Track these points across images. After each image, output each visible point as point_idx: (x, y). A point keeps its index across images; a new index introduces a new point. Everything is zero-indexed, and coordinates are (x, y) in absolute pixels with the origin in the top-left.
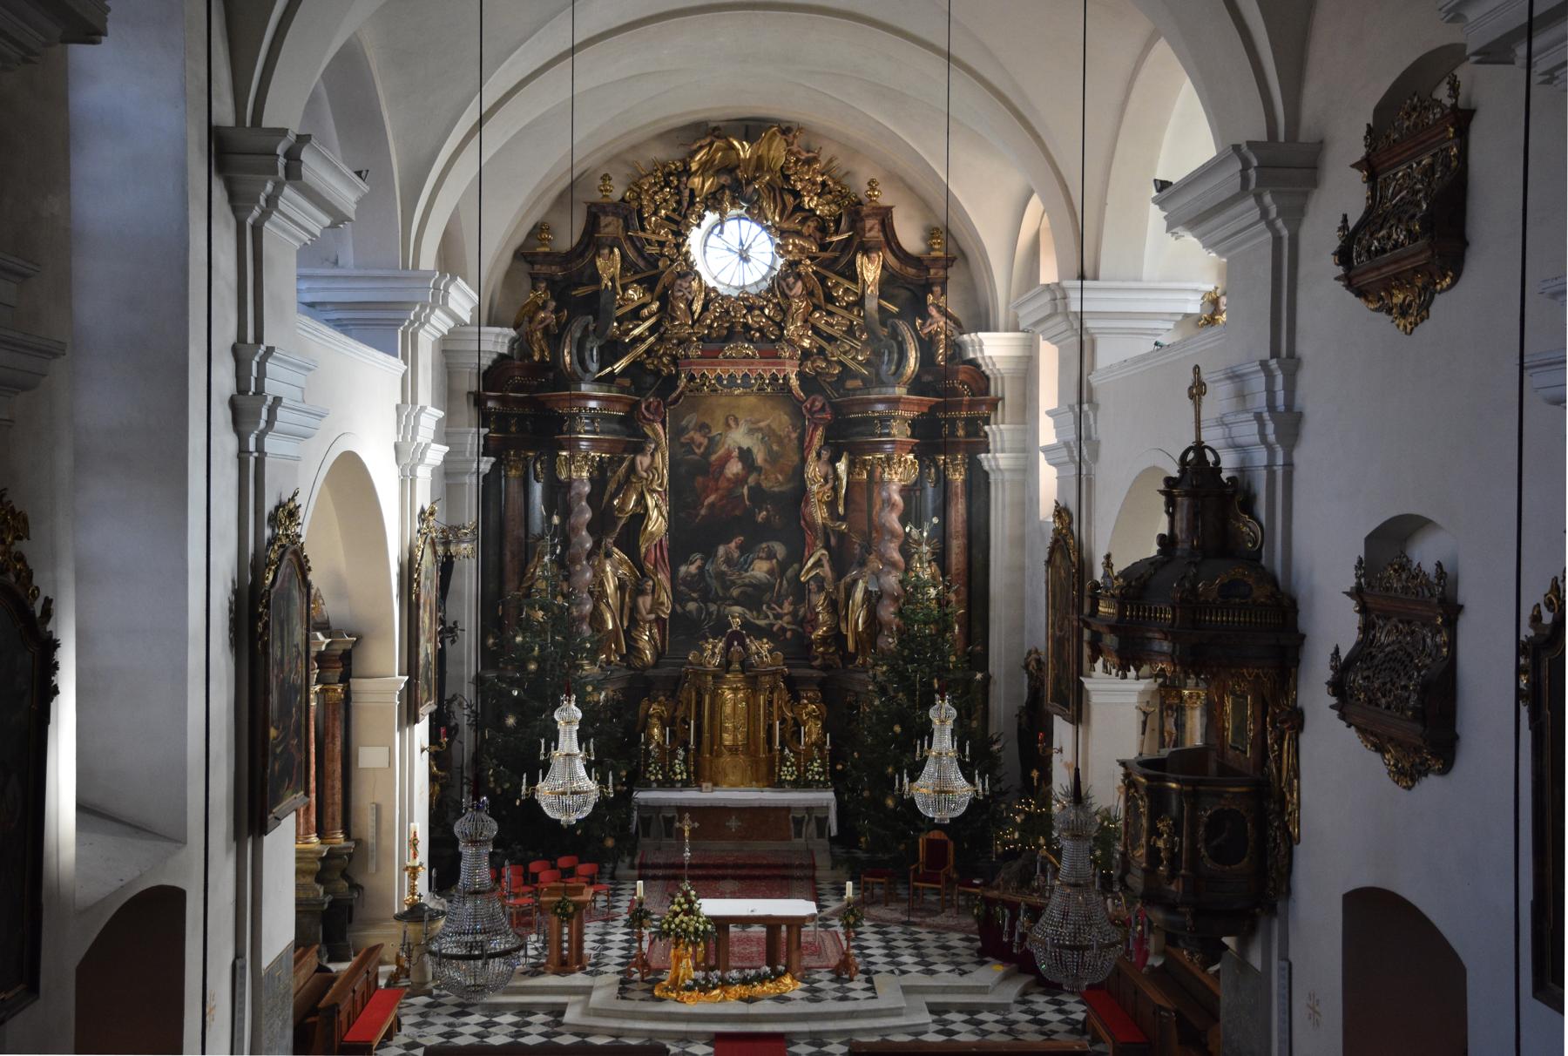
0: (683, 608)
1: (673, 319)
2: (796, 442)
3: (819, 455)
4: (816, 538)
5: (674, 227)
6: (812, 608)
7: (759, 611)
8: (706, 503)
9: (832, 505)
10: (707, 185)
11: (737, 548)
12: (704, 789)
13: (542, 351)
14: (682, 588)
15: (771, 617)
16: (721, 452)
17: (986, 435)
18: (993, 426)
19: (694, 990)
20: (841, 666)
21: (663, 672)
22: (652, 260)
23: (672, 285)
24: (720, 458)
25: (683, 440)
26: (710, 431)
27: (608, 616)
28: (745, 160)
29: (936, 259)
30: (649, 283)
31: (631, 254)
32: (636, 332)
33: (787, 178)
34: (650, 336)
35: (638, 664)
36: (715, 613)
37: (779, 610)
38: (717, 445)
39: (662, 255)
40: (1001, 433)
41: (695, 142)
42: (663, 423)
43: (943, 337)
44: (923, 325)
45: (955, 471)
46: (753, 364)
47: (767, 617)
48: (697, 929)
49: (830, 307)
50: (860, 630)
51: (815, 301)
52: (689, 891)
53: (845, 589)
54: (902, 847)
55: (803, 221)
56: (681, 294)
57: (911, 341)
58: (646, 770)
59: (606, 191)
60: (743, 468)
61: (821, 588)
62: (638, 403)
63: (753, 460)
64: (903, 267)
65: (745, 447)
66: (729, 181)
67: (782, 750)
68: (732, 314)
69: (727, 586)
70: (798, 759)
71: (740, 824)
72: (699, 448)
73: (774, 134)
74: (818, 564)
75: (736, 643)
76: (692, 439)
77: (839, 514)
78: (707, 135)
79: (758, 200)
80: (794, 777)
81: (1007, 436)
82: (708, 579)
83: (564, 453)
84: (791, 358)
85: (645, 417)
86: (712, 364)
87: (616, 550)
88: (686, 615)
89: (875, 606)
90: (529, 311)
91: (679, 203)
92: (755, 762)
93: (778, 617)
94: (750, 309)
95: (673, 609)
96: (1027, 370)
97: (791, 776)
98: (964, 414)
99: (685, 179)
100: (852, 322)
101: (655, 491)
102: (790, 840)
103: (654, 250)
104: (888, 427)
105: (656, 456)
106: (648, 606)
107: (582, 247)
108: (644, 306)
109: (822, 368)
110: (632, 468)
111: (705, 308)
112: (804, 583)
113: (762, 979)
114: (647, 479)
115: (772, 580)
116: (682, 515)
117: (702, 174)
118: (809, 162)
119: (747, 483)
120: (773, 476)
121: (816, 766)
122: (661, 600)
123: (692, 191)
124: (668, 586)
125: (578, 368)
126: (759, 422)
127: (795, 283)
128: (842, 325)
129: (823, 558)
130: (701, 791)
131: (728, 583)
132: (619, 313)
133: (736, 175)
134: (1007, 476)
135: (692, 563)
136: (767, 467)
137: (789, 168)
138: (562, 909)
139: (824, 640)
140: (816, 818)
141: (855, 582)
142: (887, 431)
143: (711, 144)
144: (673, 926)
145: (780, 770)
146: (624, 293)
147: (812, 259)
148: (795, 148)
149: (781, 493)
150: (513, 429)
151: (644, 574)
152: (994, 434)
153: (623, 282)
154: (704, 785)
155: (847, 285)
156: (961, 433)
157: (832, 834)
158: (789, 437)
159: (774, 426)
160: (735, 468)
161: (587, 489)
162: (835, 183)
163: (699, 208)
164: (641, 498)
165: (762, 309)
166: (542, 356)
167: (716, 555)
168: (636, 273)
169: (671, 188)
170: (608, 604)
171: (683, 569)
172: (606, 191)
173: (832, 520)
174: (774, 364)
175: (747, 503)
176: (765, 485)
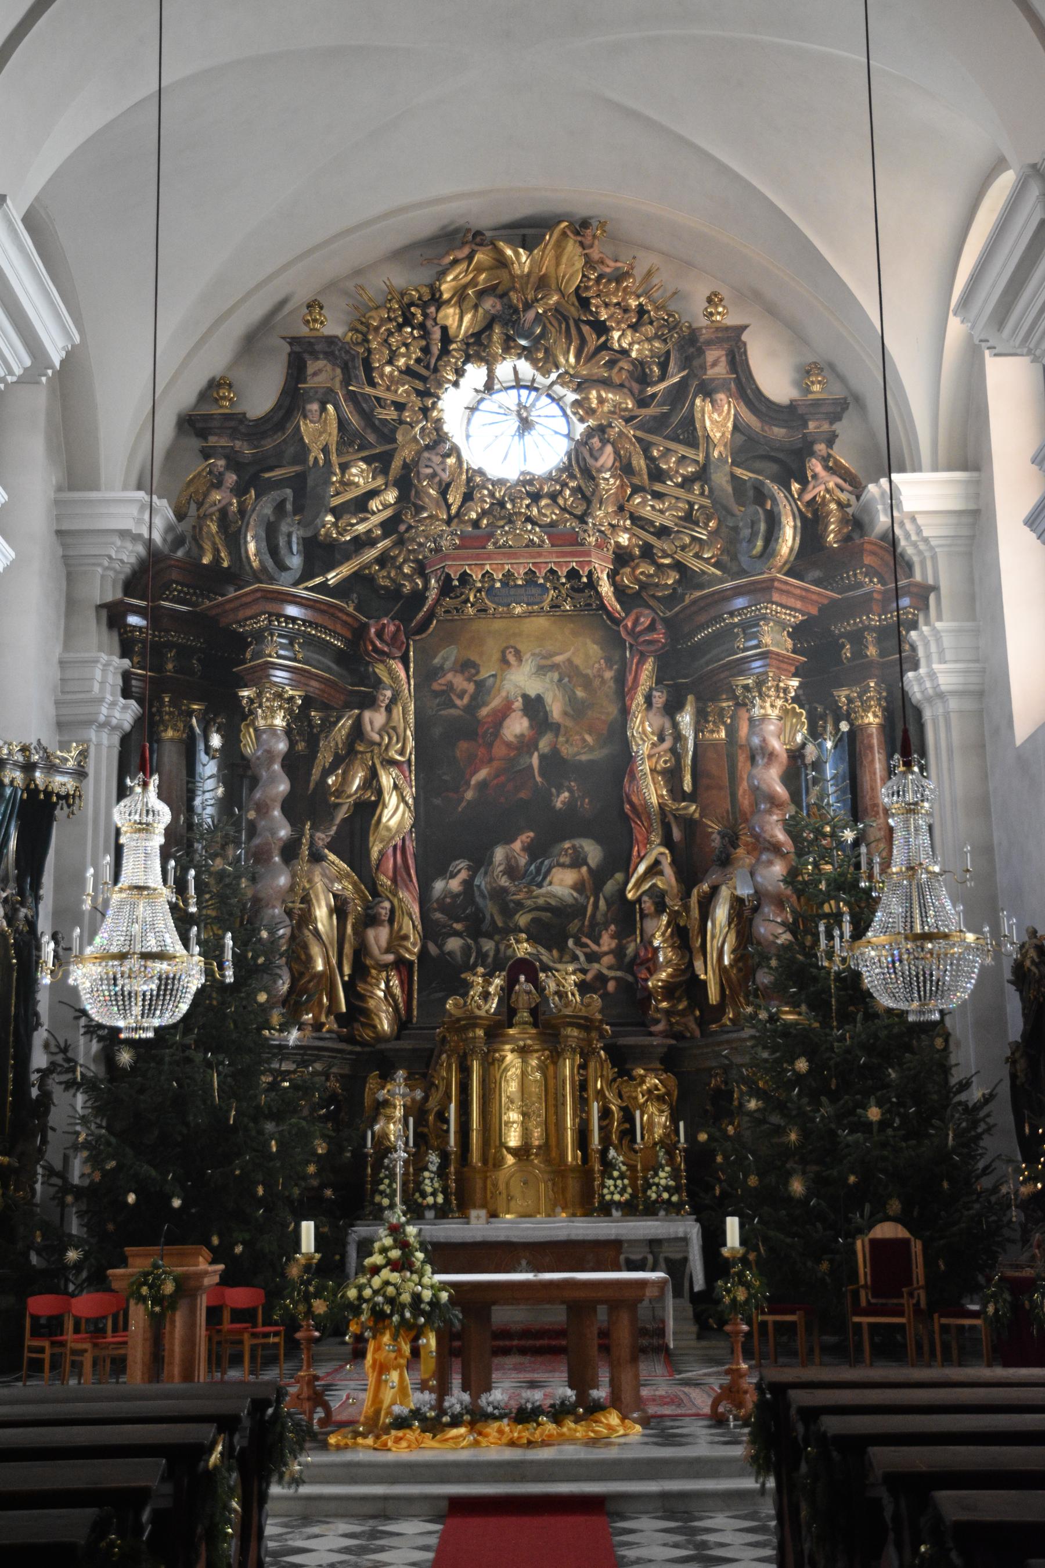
1: (419, 509)
2: (612, 684)
3: (649, 700)
4: (649, 832)
5: (420, 386)
6: (647, 942)
7: (562, 949)
8: (473, 782)
9: (672, 776)
10: (467, 318)
12: (473, 1220)
13: (216, 551)
14: (438, 915)
15: (582, 958)
16: (496, 703)
17: (913, 648)
18: (925, 629)
19: (410, 1427)
20: (698, 1033)
21: (405, 1044)
22: (386, 431)
23: (416, 462)
24: (494, 712)
25: (435, 686)
26: (478, 672)
27: (316, 950)
28: (522, 277)
29: (817, 403)
30: (381, 462)
31: (354, 421)
32: (361, 528)
33: (585, 303)
34: (385, 536)
35: (367, 1035)
36: (492, 954)
37: (594, 947)
38: (489, 692)
39: (401, 422)
40: (938, 640)
41: (447, 253)
42: (405, 661)
43: (833, 506)
44: (801, 492)
45: (867, 709)
46: (540, 555)
47: (575, 958)
48: (417, 1298)
49: (658, 487)
50: (726, 962)
51: (636, 481)
52: (403, 1225)
53: (699, 902)
54: (825, 1266)
55: (611, 364)
56: (429, 471)
57: (785, 502)
58: (375, 1191)
59: (315, 321)
60: (531, 726)
61: (661, 907)
62: (365, 627)
63: (546, 713)
64: (766, 428)
65: (532, 694)
66: (499, 307)
67: (604, 1152)
68: (509, 506)
69: (509, 910)
70: (632, 1168)
72: (461, 697)
73: (564, 234)
74: (654, 869)
75: (522, 978)
76: (450, 685)
77: (684, 792)
78: (464, 244)
79: (542, 335)
80: (626, 1196)
81: (947, 641)
82: (479, 900)
83: (246, 694)
84: (598, 546)
85: (376, 649)
86: (478, 557)
87: (332, 857)
88: (445, 957)
89: (751, 920)
90: (196, 492)
91: (426, 350)
92: (558, 1170)
93: (593, 957)
94: (536, 497)
95: (423, 954)
96: (972, 537)
98: (875, 620)
99: (432, 309)
100: (691, 505)
101: (393, 763)
103: (391, 414)
104: (755, 636)
105: (395, 712)
107: (281, 413)
108: (373, 494)
109: (649, 576)
110: (357, 731)
111: (468, 497)
112: (632, 903)
113: (559, 1413)
114: (379, 745)
115: (581, 900)
116: (437, 801)
117: (460, 303)
118: (619, 277)
119: (537, 749)
120: (577, 737)
121: (663, 1177)
122: (403, 932)
123: (444, 329)
124: (415, 909)
125: (270, 563)
127: (601, 449)
128: (678, 509)
129: (662, 859)
131: (512, 905)
132: (335, 502)
133: (510, 300)
134: (953, 704)
135: (453, 876)
136: (569, 723)
137: (587, 288)
138: (151, 1287)
139: (669, 990)
141: (715, 890)
142: (754, 642)
143: (470, 258)
144: (367, 1293)
145: (603, 1186)
146: (343, 472)
147: (628, 420)
148: (595, 254)
149: (591, 762)
150: (170, 666)
151: (375, 894)
152: (927, 644)
153: (344, 460)
154: (473, 1213)
155: (682, 450)
156: (872, 651)
157: (697, 1289)
158: (602, 677)
159: (578, 661)
160: (517, 726)
161: (282, 746)
162: (657, 309)
163: (456, 357)
164: (372, 780)
165: (554, 497)
166: (217, 559)
167: (491, 863)
168: (361, 448)
169: (413, 328)
170: (316, 933)
171: (439, 886)
172: (315, 321)
173: (674, 800)
174: (573, 554)
175: (539, 779)
176: (566, 751)
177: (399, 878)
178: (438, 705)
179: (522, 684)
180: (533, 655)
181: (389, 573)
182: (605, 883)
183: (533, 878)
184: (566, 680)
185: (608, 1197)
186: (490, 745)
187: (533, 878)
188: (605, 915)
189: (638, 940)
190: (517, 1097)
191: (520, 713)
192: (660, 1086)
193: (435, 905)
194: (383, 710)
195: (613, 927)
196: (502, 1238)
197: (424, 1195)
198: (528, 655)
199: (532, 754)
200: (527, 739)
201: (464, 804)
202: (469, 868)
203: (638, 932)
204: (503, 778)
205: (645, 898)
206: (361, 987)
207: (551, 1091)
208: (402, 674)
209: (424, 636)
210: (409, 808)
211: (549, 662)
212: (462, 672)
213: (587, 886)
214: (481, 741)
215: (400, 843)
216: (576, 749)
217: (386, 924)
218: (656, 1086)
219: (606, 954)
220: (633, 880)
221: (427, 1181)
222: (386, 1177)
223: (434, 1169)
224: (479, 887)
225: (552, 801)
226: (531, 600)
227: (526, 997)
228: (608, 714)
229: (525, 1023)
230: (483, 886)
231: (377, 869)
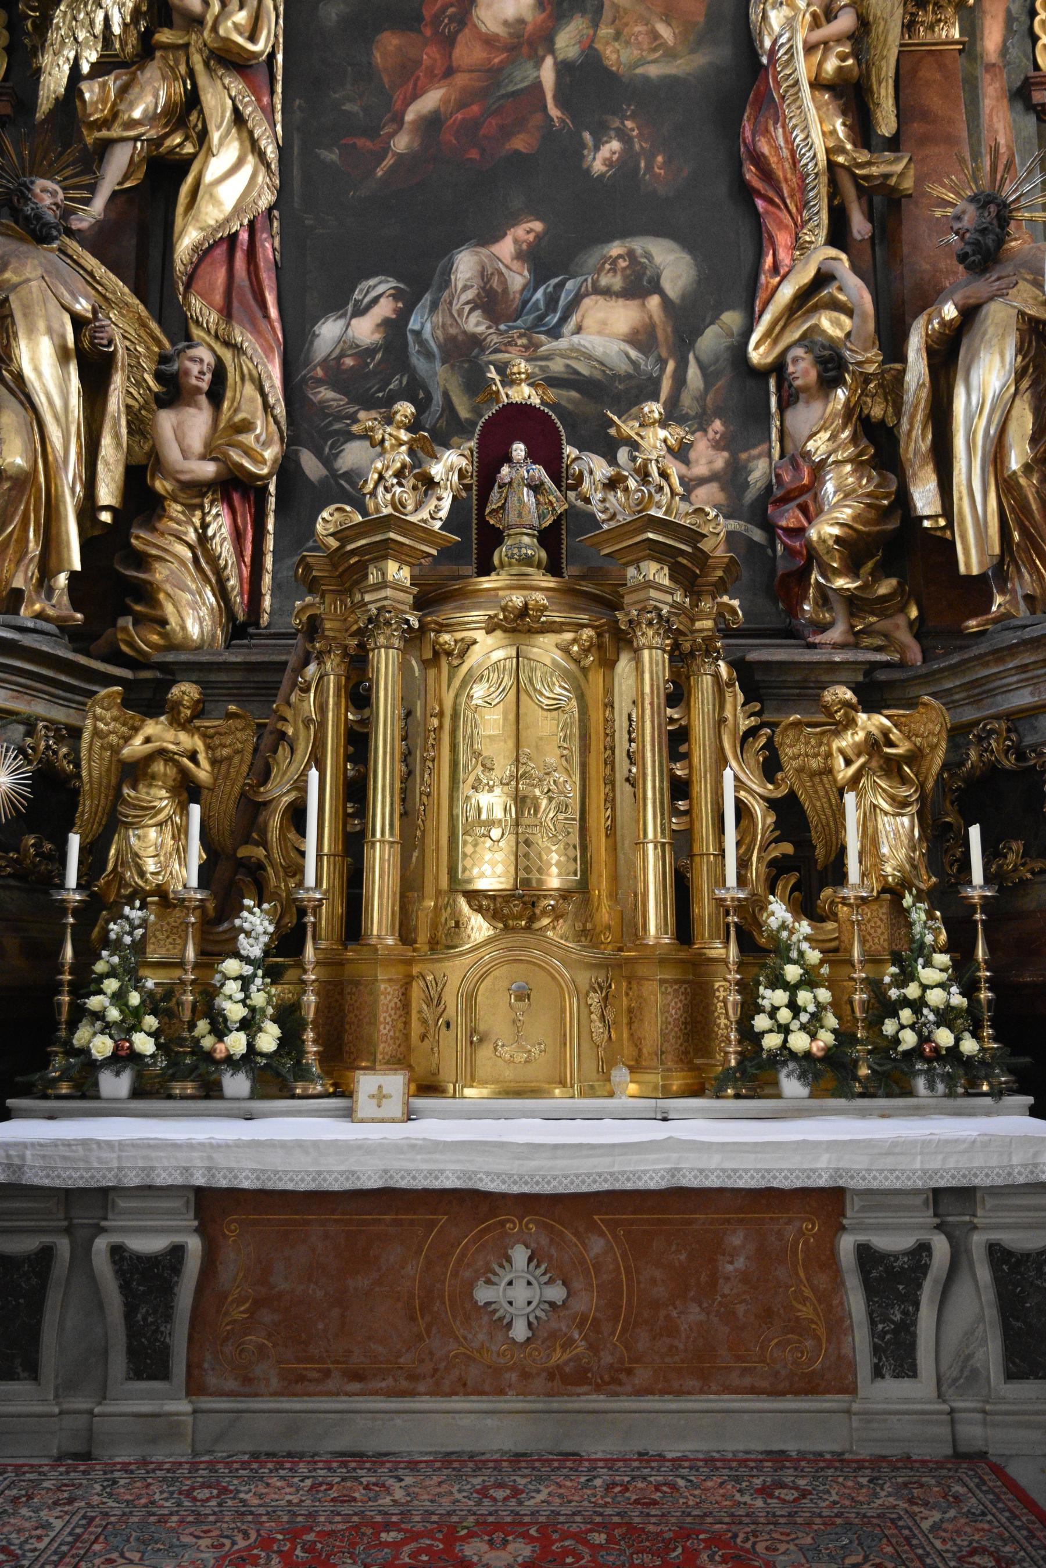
0: (328, 462)
8: (410, 116)
11: (519, 256)
12: (364, 1103)
14: (326, 394)
20: (915, 654)
50: (1015, 463)
58: (79, 1014)
71: (556, 1293)
75: (519, 450)
80: (826, 1038)
82: (419, 363)
97: (811, 1030)
102: (851, 1390)
106: (196, 441)
112: (760, 374)
115: (648, 365)
116: (332, 156)
119: (551, 50)
120: (639, 28)
124: (274, 373)
130: (349, 1114)
135: (360, 311)
140: (997, 1254)
141: (969, 314)
145: (750, 1007)
149: (670, 83)
154: (366, 1083)
167: (446, 283)
175: (554, 112)
177: (235, 304)
182: (700, 332)
183: (541, 318)
185: (772, 1041)
186: (449, 42)
187: (541, 318)
188: (701, 398)
189: (776, 453)
190: (501, 754)
192: (895, 735)
193: (320, 372)
195: (717, 425)
196: (450, 1182)
197: (220, 1029)
199: (543, 59)
200: (529, 28)
201: (389, 161)
202: (397, 295)
203: (774, 434)
204: (475, 108)
205: (799, 352)
206: (140, 539)
207: (597, 744)
210: (268, 166)
213: (660, 335)
214: (428, 32)
215: (244, 236)
216: (636, 52)
217: (203, 399)
218: (886, 733)
219: (702, 481)
221: (232, 988)
222: (112, 973)
223: (256, 951)
224: (418, 334)
225: (582, 157)
227: (528, 497)
229: (527, 561)
230: (427, 334)
231: (188, 286)
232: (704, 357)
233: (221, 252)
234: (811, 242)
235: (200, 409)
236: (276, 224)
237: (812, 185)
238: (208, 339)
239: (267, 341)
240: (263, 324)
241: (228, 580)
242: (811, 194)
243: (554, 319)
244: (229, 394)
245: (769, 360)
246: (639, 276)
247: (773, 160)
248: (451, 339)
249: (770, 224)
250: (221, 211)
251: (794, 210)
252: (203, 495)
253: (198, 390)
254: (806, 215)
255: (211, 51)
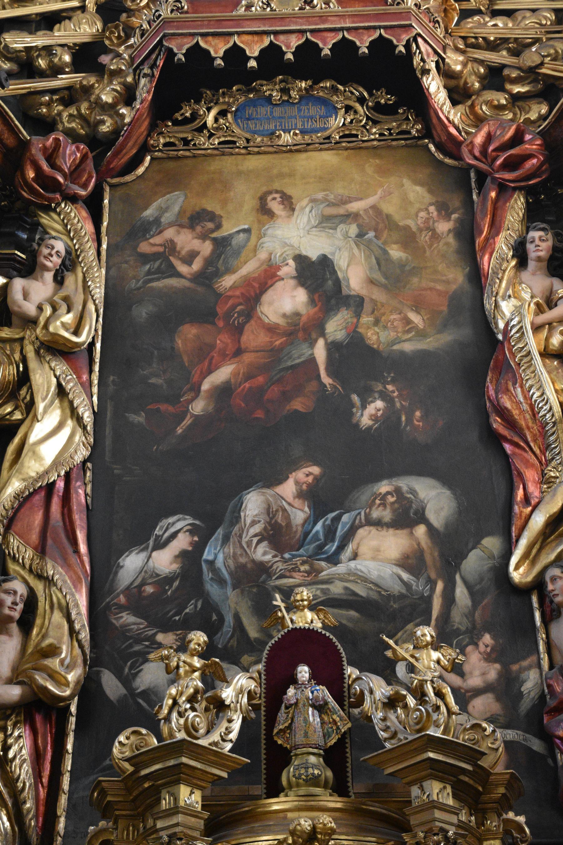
2: (451, 239)
8: (206, 386)
11: (300, 495)
24: (247, 281)
25: (144, 247)
26: (219, 227)
38: (237, 253)
60: (312, 301)
63: (337, 283)
65: (313, 255)
76: (171, 246)
82: (212, 589)
115: (419, 586)
116: (139, 419)
119: (323, 334)
120: (394, 316)
126: (350, 200)
135: (160, 545)
136: (379, 295)
149: (423, 355)
159: (389, 208)
167: (236, 519)
175: (327, 380)
177: (50, 542)
178: (149, 273)
179: (294, 241)
180: (313, 201)
181: (79, 110)
182: (464, 556)
183: (320, 547)
184: (371, 234)
186: (239, 330)
187: (320, 547)
188: (470, 615)
191: (292, 282)
193: (122, 599)
194: (49, 276)
195: (487, 639)
198: (305, 202)
199: (316, 341)
200: (304, 319)
201: (187, 421)
203: (542, 647)
204: (260, 379)
208: (89, 227)
209: (129, 178)
210: (84, 428)
211: (341, 211)
212: (192, 227)
213: (428, 558)
214: (221, 324)
215: (61, 485)
216: (393, 334)
217: (14, 628)
219: (478, 692)
220: (523, 543)
224: (211, 563)
225: (352, 414)
226: (309, 125)
227: (313, 717)
228: (448, 282)
229: (314, 781)
230: (220, 563)
232: (470, 578)
233: (39, 499)
234: (557, 477)
235: (10, 635)
236: (89, 474)
237: (551, 432)
238: (22, 572)
239: (76, 573)
240: (73, 559)
241: (25, 802)
242: (552, 438)
243: (332, 547)
244: (38, 621)
245: (529, 579)
246: (406, 510)
247: (515, 412)
248: (241, 567)
249: (518, 463)
250: (42, 465)
251: (538, 452)
252: (7, 718)
253: (10, 619)
254: (549, 455)
255: (42, 343)
